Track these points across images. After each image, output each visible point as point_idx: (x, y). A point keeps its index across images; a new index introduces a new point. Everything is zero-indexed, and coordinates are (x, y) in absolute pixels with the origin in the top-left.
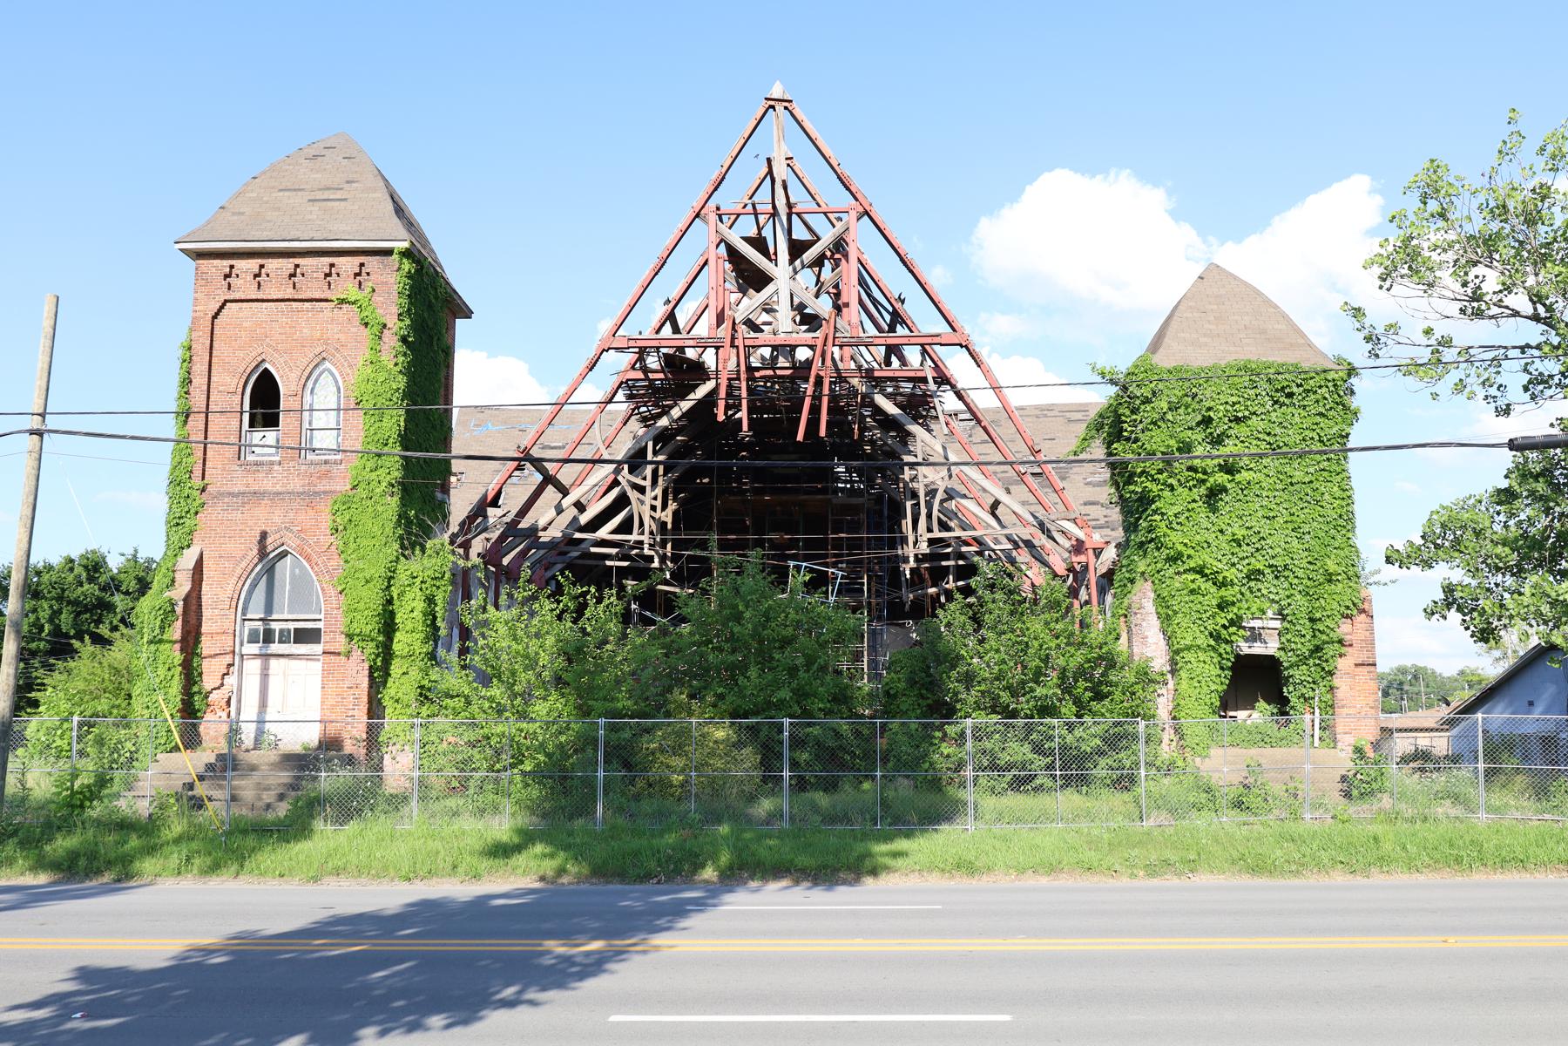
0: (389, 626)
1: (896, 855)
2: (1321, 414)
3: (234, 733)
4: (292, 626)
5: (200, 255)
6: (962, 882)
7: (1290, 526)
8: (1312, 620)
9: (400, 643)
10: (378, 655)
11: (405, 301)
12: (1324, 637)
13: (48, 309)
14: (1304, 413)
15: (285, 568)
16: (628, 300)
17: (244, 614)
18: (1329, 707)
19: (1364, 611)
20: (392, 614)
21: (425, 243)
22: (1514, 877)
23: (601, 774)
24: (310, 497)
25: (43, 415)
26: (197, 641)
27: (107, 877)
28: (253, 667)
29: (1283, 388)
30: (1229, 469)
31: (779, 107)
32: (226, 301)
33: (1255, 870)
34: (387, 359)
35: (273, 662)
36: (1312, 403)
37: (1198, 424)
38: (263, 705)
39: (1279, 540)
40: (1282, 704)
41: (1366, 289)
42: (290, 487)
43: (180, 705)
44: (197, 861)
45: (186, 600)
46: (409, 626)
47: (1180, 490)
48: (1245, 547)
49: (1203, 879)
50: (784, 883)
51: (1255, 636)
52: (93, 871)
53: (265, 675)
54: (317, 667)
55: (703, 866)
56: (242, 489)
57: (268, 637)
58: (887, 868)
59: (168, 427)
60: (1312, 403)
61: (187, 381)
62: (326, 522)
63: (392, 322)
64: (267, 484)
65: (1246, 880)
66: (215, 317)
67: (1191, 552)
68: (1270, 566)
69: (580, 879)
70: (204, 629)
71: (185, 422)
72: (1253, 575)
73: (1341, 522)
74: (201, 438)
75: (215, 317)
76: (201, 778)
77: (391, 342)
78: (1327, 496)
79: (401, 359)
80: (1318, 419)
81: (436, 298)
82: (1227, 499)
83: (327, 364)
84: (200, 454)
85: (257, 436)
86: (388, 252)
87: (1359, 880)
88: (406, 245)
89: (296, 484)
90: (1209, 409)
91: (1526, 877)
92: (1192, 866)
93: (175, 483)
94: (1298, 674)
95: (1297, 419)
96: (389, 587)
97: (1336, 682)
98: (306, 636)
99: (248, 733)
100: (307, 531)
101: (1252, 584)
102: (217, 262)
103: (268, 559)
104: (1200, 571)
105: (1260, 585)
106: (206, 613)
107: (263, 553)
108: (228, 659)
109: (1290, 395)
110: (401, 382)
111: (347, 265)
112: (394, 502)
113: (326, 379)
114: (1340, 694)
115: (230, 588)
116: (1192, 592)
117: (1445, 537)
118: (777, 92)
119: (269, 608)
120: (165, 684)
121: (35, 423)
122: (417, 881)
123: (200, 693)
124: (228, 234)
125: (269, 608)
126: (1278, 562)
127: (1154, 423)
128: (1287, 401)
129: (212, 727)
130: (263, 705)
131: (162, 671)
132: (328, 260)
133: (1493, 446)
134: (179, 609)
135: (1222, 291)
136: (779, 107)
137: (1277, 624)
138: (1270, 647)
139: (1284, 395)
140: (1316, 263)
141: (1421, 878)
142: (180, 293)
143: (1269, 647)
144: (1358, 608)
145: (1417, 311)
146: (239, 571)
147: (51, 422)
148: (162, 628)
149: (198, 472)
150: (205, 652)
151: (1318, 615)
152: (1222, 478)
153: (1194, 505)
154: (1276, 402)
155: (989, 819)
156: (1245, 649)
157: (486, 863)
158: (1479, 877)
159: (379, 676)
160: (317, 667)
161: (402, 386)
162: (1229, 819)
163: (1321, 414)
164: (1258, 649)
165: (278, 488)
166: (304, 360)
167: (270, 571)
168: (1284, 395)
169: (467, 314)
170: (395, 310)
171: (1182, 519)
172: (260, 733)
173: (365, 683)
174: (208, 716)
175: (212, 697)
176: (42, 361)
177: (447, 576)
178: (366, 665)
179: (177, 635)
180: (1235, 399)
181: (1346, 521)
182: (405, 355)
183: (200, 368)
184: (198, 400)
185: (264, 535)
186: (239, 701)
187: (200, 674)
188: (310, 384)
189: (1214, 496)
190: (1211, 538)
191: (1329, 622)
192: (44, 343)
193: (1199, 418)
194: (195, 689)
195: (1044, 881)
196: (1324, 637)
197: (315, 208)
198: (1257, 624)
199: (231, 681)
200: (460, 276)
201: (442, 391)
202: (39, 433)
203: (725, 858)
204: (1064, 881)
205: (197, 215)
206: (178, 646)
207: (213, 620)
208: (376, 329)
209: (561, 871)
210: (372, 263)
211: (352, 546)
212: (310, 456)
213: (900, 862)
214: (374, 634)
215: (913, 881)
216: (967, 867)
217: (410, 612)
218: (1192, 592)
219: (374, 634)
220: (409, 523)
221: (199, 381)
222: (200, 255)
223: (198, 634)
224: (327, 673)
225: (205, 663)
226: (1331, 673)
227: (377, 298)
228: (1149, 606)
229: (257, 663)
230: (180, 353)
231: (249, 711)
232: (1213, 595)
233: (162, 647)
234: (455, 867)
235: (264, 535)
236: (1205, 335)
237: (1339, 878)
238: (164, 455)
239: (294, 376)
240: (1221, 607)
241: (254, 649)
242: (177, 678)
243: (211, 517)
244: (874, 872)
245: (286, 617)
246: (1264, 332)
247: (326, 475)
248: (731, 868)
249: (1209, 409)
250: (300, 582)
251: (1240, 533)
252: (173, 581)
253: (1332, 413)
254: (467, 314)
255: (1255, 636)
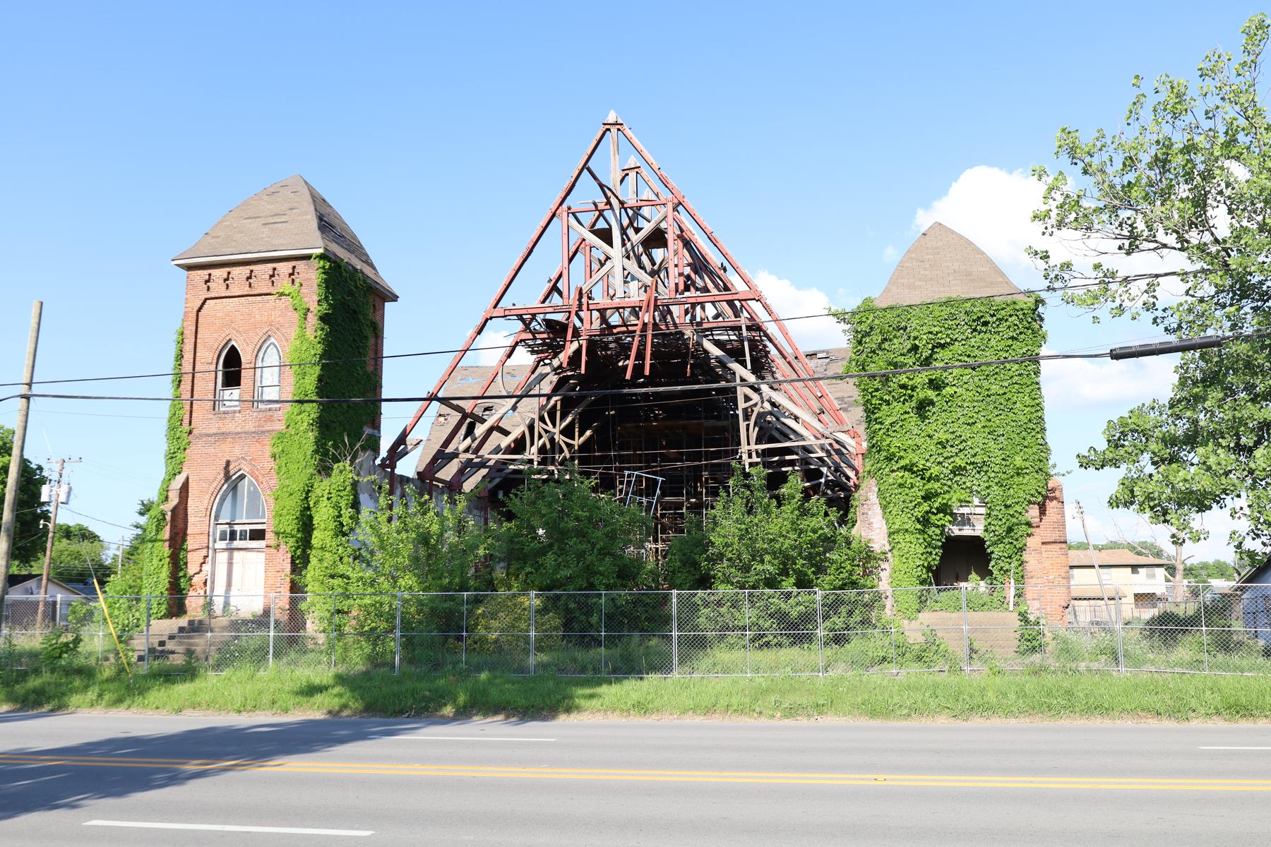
0: (306, 524)
1: (592, 696)
2: (1013, 338)
3: (209, 605)
4: (248, 528)
5: (190, 268)
6: (637, 720)
7: (987, 430)
8: (1007, 507)
9: (317, 538)
10: (298, 548)
11: (323, 291)
12: (1014, 520)
13: (35, 311)
14: (998, 338)
15: (245, 486)
16: (505, 281)
17: (217, 518)
18: (1021, 579)
19: (1055, 498)
20: (311, 518)
21: (355, 247)
22: (1097, 722)
23: (272, 634)
24: (259, 434)
25: (30, 385)
26: (184, 540)
27: (47, 708)
28: (222, 557)
29: (979, 318)
30: (935, 385)
31: (614, 130)
32: (206, 299)
33: (873, 714)
34: (310, 334)
35: (236, 554)
36: (1012, 327)
37: (910, 351)
38: (229, 584)
39: (978, 440)
40: (985, 573)
41: (1034, 236)
42: (246, 429)
43: (167, 586)
44: (106, 697)
45: (174, 511)
46: (323, 526)
47: (895, 404)
48: (949, 449)
49: (829, 720)
50: (501, 717)
51: (965, 520)
52: (38, 704)
53: (230, 564)
54: (262, 556)
55: (445, 705)
56: (216, 431)
57: (233, 536)
58: (578, 709)
59: (166, 388)
60: (1012, 327)
61: (180, 357)
62: (268, 451)
63: (314, 307)
64: (231, 426)
65: (864, 722)
66: (199, 311)
67: (902, 453)
68: (973, 463)
69: (355, 714)
70: (189, 531)
71: (179, 386)
72: (957, 471)
73: (1031, 425)
74: (211, 397)
75: (199, 311)
76: (171, 637)
77: (313, 320)
78: (1018, 405)
79: (319, 333)
80: (1010, 342)
81: (356, 287)
82: (934, 410)
83: (272, 340)
84: (188, 408)
85: (227, 393)
86: (308, 257)
87: (959, 723)
88: (321, 251)
89: (250, 427)
90: (915, 338)
91: (1107, 723)
92: (819, 708)
93: (172, 428)
94: (997, 551)
95: (993, 342)
96: (306, 498)
97: (1025, 557)
98: (258, 535)
99: (218, 604)
100: (257, 461)
101: (958, 478)
102: (200, 272)
103: (232, 481)
104: (909, 468)
105: (964, 479)
106: (191, 519)
107: (227, 476)
108: (204, 552)
109: (986, 324)
110: (319, 349)
111: (284, 268)
112: (311, 436)
113: (272, 350)
114: (1029, 567)
115: (206, 502)
116: (901, 486)
117: (1124, 439)
118: (611, 118)
119: (233, 516)
120: (157, 572)
121: (23, 390)
122: (244, 714)
123: (185, 576)
124: (206, 252)
125: (233, 516)
126: (978, 459)
127: (874, 352)
128: (984, 329)
129: (194, 603)
130: (229, 584)
131: (155, 562)
132: (271, 266)
133: (1096, 356)
134: (168, 517)
135: (940, 244)
136: (614, 130)
137: (983, 510)
138: (977, 529)
139: (980, 324)
140: (998, 217)
141: (1013, 721)
142: (179, 293)
143: (977, 529)
144: (1046, 499)
145: (1067, 246)
146: (211, 489)
147: (36, 389)
148: (157, 531)
149: (186, 421)
150: (190, 548)
151: (1009, 503)
152: (931, 394)
153: (906, 416)
154: (975, 330)
155: (733, 668)
156: (956, 531)
157: (299, 699)
158: (1065, 722)
159: (299, 563)
160: (261, 557)
161: (319, 352)
162: (915, 668)
163: (1013, 338)
164: (967, 531)
165: (239, 430)
166: (256, 339)
167: (234, 488)
168: (980, 324)
169: (394, 298)
170: (316, 298)
171: (897, 427)
172: (227, 604)
173: (288, 568)
174: (191, 593)
175: (195, 579)
176: (30, 346)
177: (349, 488)
178: (289, 555)
179: (167, 536)
180: (937, 329)
181: (1036, 425)
182: (322, 329)
183: (189, 347)
184: (187, 367)
185: (228, 463)
186: (213, 582)
187: (186, 564)
188: (261, 354)
189: (923, 407)
190: (919, 441)
191: (1018, 508)
192: (32, 334)
193: (909, 346)
194: (181, 574)
195: (699, 720)
196: (1014, 520)
197: (266, 230)
198: (965, 510)
199: (207, 567)
200: (387, 270)
201: (371, 354)
202: (27, 398)
203: (462, 699)
204: (716, 720)
205: (190, 238)
206: (167, 544)
207: (196, 524)
208: (301, 313)
209: (345, 706)
210: (301, 265)
211: (284, 469)
212: (261, 406)
213: (594, 702)
214: (294, 532)
215: (599, 719)
216: (641, 707)
217: (323, 515)
218: (901, 486)
219: (294, 532)
220: (325, 454)
221: (188, 356)
222: (190, 268)
223: (185, 534)
224: (269, 561)
225: (190, 555)
226: (1022, 549)
227: (304, 290)
228: (873, 498)
229: (226, 554)
230: (175, 337)
231: (220, 589)
232: (919, 488)
233: (157, 544)
234: (274, 702)
235: (228, 463)
236: (920, 280)
237: (943, 721)
238: (164, 409)
239: (250, 349)
240: (927, 497)
241: (221, 545)
242: (166, 566)
243: (196, 450)
244: (568, 710)
245: (244, 523)
246: (970, 274)
247: (270, 419)
248: (465, 707)
249: (915, 338)
250: (254, 496)
251: (944, 437)
252: (167, 497)
253: (1022, 336)
254: (394, 298)
255: (965, 520)
